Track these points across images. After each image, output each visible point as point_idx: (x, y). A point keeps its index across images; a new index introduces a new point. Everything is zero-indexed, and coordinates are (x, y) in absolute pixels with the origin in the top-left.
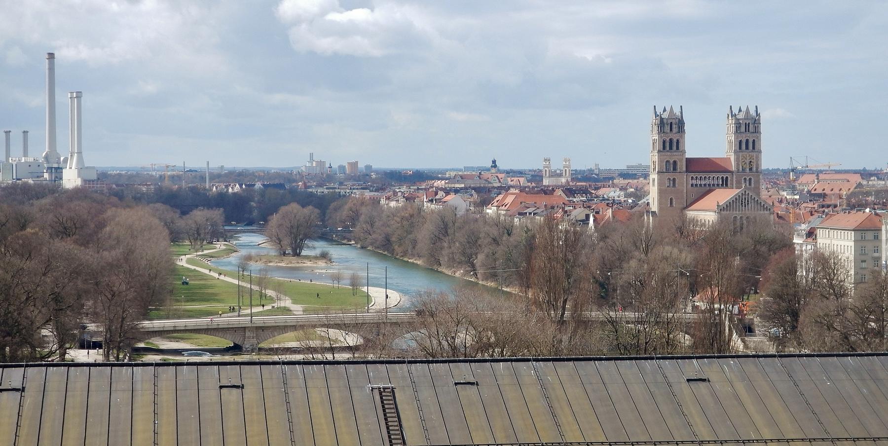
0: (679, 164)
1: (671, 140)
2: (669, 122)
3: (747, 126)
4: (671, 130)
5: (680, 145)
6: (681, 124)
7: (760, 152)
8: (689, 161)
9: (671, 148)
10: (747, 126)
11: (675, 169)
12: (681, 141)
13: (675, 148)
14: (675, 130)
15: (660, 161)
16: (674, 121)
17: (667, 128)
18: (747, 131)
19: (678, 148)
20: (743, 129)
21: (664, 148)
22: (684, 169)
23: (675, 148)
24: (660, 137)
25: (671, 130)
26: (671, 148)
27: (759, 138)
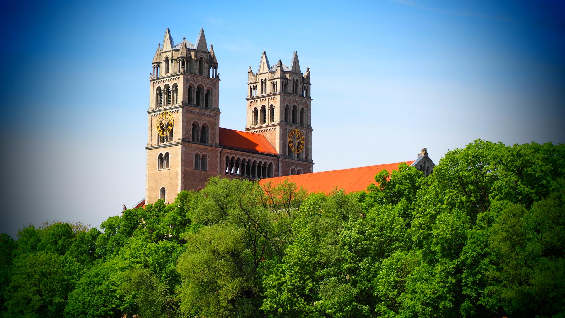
0: (210, 131)
2: (200, 55)
3: (295, 83)
7: (310, 129)
8: (221, 129)
9: (198, 104)
10: (295, 83)
15: (186, 122)
16: (205, 56)
17: (196, 67)
19: (207, 106)
20: (290, 89)
21: (190, 99)
22: (217, 142)
24: (186, 81)
26: (198, 104)
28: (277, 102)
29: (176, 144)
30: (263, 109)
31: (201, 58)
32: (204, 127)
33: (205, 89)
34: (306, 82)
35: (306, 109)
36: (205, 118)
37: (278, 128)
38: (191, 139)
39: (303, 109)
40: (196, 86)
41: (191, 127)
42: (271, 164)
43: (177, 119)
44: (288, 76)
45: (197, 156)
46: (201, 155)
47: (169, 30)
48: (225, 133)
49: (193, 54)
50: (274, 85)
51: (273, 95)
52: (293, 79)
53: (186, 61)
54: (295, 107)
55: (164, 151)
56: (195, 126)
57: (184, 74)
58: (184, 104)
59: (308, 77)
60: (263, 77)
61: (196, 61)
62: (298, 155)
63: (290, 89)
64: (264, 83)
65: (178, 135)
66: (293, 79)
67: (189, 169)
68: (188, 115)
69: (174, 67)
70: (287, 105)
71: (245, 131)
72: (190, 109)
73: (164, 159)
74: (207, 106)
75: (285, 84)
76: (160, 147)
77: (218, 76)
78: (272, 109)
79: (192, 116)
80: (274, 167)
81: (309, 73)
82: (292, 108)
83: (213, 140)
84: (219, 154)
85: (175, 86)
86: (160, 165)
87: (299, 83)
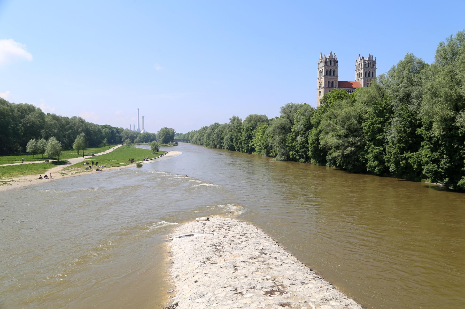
0: (335, 83)
1: (331, 70)
2: (330, 59)
4: (331, 65)
5: (335, 73)
6: (336, 61)
8: (339, 82)
9: (330, 75)
10: (369, 64)
11: (332, 86)
12: (336, 71)
13: (332, 74)
14: (333, 64)
17: (329, 64)
18: (369, 67)
19: (334, 75)
20: (367, 66)
22: (338, 86)
23: (332, 74)
25: (331, 65)
26: (330, 75)
27: (375, 71)
28: (362, 71)
32: (333, 82)
34: (374, 63)
43: (323, 80)
44: (366, 62)
48: (340, 83)
51: (361, 68)
53: (326, 62)
56: (329, 82)
57: (324, 66)
58: (324, 76)
59: (375, 61)
60: (359, 63)
63: (367, 66)
64: (359, 65)
69: (322, 64)
72: (326, 77)
73: (320, 92)
74: (334, 75)
75: (365, 64)
77: (337, 65)
82: (368, 72)
83: (336, 86)
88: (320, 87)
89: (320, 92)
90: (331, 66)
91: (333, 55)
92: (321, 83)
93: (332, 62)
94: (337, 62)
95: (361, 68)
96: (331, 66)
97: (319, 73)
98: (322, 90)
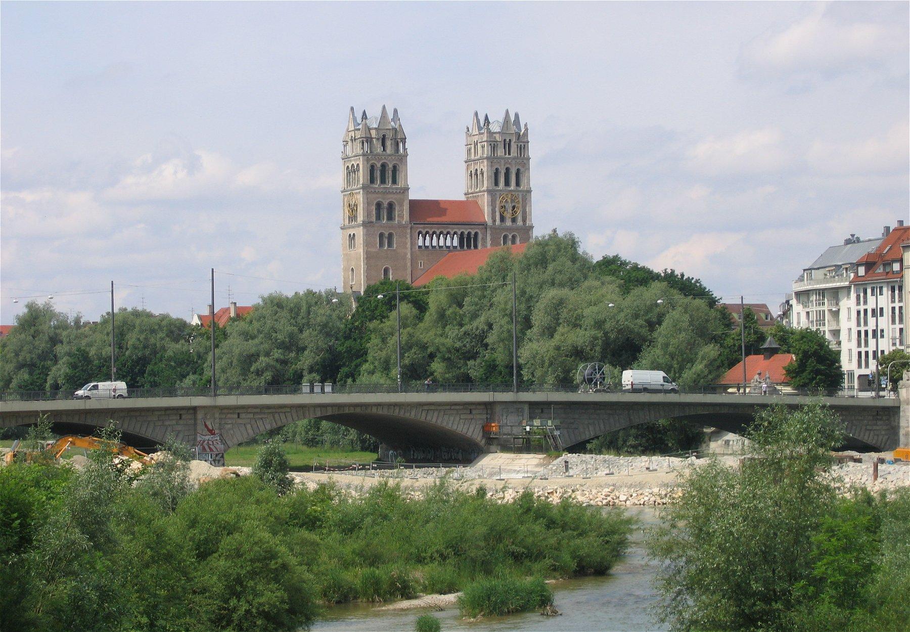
0: (397, 208)
12: (400, 167)
15: (368, 203)
18: (506, 156)
19: (394, 181)
21: (372, 180)
28: (484, 166)
29: (358, 226)
30: (476, 174)
31: (384, 136)
33: (391, 166)
35: (522, 170)
36: (390, 196)
37: (486, 194)
38: (374, 219)
39: (518, 170)
40: (379, 165)
41: (374, 207)
42: (476, 234)
43: (360, 198)
45: (381, 235)
46: (387, 234)
47: (352, 109)
48: (415, 205)
49: (373, 133)
50: (483, 147)
52: (505, 140)
54: (508, 169)
55: (352, 232)
56: (379, 206)
60: (476, 139)
61: (378, 139)
62: (514, 220)
64: (476, 144)
65: (360, 219)
66: (505, 140)
67: (373, 250)
68: (370, 195)
70: (497, 169)
71: (463, 198)
76: (349, 228)
77: (405, 149)
78: (482, 174)
79: (374, 196)
80: (480, 236)
81: (527, 130)
84: (409, 231)
85: (358, 165)
86: (350, 246)
87: (512, 143)
88: (353, 217)
89: (352, 238)
90: (381, 155)
91: (390, 116)
92: (353, 209)
93: (388, 143)
94: (404, 140)
95: (482, 158)
96: (381, 155)
97: (349, 173)
98: (360, 232)
